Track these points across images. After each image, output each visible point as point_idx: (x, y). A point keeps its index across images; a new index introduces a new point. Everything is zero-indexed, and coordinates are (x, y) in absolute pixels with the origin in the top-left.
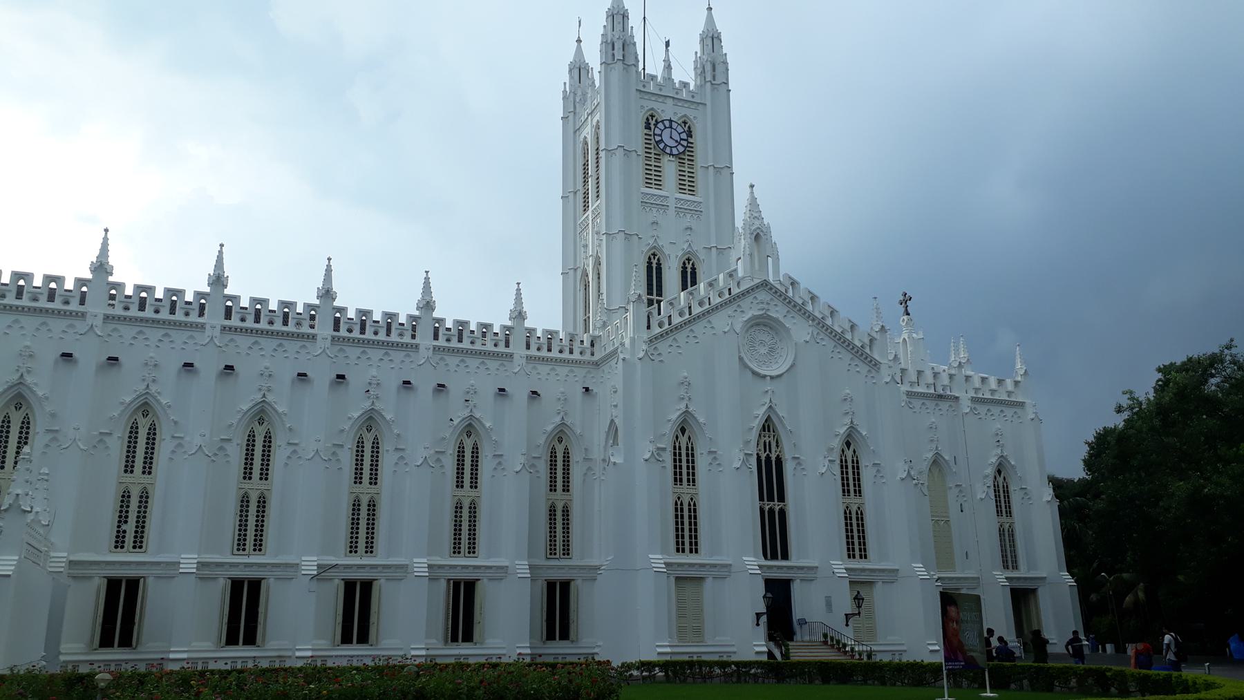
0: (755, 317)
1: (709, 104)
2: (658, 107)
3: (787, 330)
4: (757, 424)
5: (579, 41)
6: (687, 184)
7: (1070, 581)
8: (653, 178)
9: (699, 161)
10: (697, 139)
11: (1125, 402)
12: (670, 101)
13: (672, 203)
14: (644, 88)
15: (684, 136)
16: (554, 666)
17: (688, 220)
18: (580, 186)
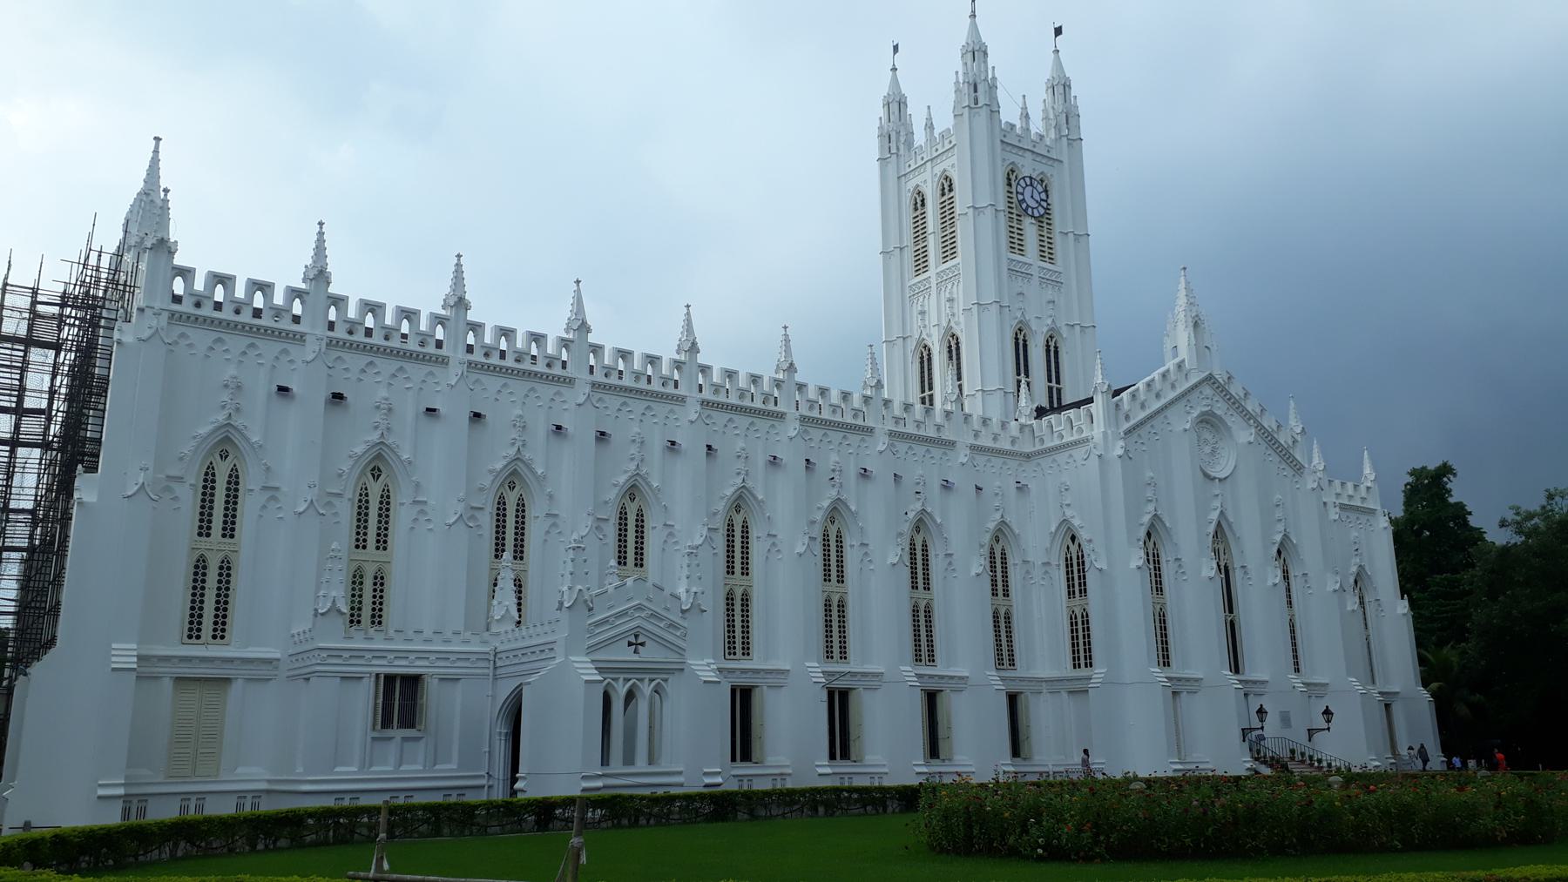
0: (1203, 414)
1: (1066, 161)
2: (1019, 161)
3: (1228, 429)
4: (1211, 529)
5: (894, 69)
6: (1047, 251)
7: (1425, 695)
8: (1017, 245)
9: (1057, 226)
10: (1054, 199)
11: (1510, 516)
12: (1028, 154)
13: (1034, 271)
14: (1009, 141)
15: (1043, 196)
16: (1038, 785)
17: (1049, 293)
18: (908, 239)
